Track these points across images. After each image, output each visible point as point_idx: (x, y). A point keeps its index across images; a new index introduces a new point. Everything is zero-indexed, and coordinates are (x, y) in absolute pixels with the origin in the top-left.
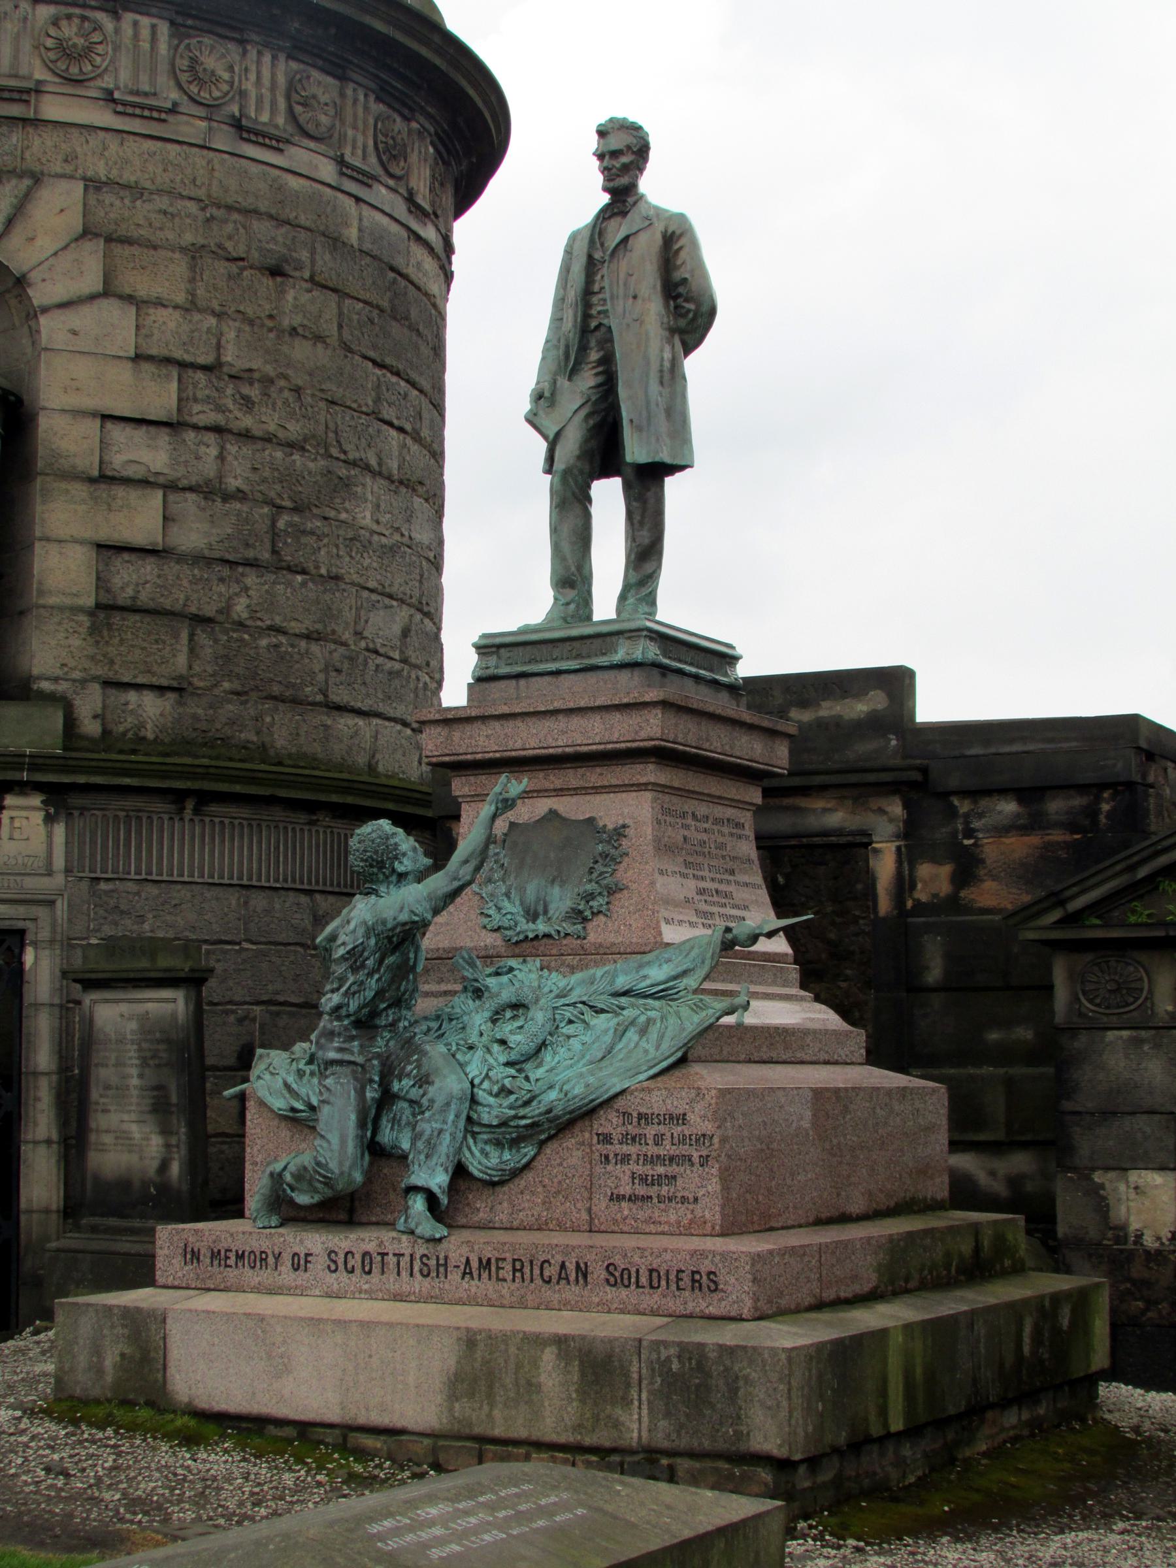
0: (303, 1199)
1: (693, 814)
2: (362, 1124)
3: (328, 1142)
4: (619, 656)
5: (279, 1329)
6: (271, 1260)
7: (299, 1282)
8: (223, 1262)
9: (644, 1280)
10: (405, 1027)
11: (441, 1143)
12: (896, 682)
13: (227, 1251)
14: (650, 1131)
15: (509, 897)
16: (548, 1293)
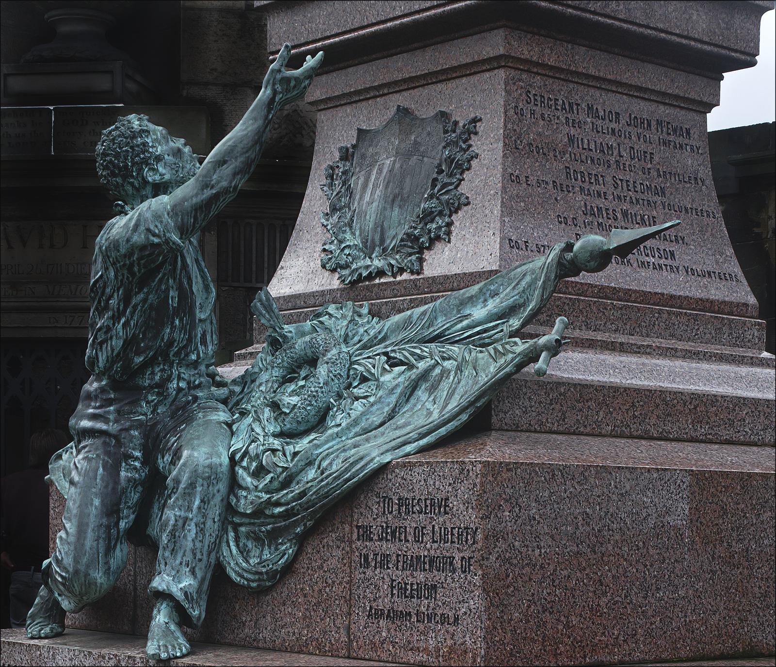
1: (590, 108)
2: (112, 510)
10: (180, 390)
11: (185, 537)
14: (410, 524)
15: (351, 227)
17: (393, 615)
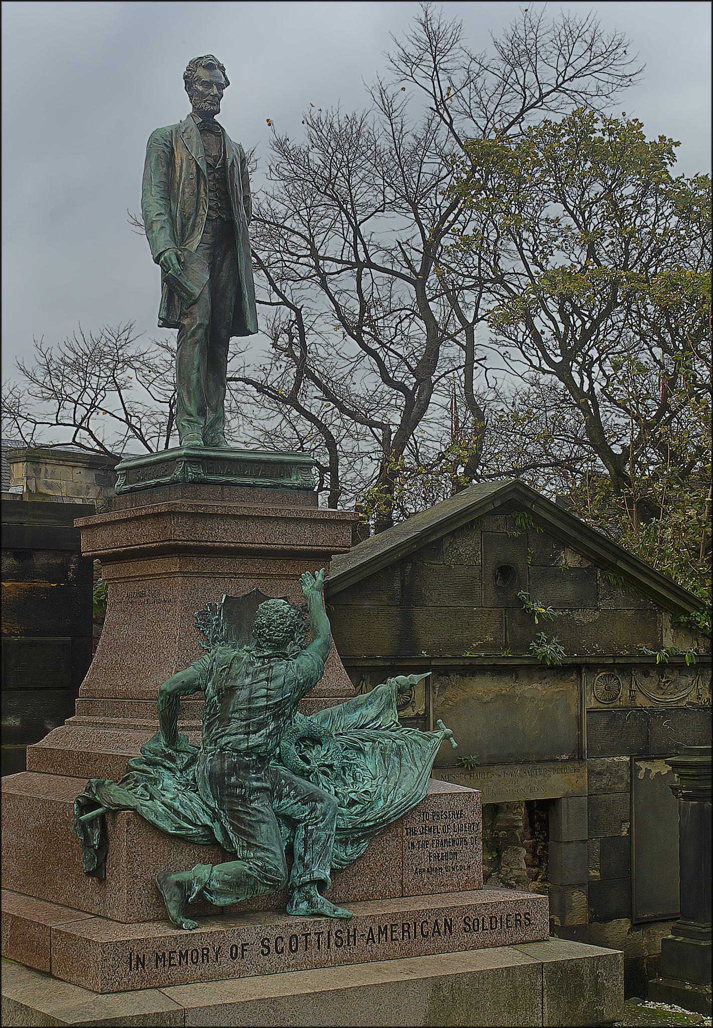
0: (220, 901)
3: (274, 853)
4: (296, 480)
5: (287, 1006)
6: (212, 954)
7: (237, 967)
8: (167, 963)
9: (487, 925)
13: (170, 953)
14: (440, 824)
16: (427, 945)
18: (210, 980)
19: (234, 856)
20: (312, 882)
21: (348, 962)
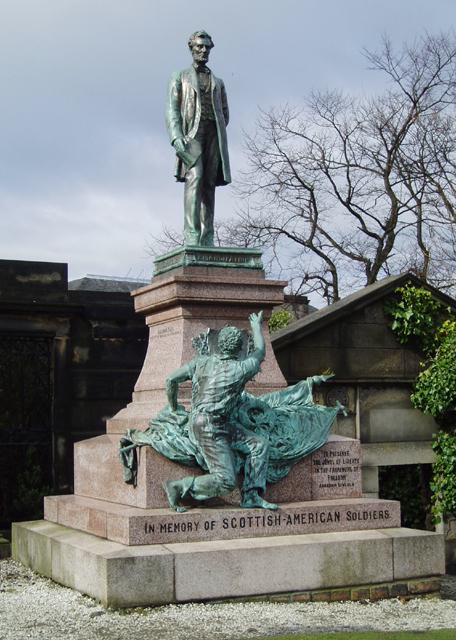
4: (252, 263)
6: (194, 526)
9: (361, 517)
12: (62, 269)
14: (335, 459)
16: (323, 526)
17: (329, 486)
18: (193, 540)
19: (207, 472)
20: (254, 488)
21: (274, 535)
